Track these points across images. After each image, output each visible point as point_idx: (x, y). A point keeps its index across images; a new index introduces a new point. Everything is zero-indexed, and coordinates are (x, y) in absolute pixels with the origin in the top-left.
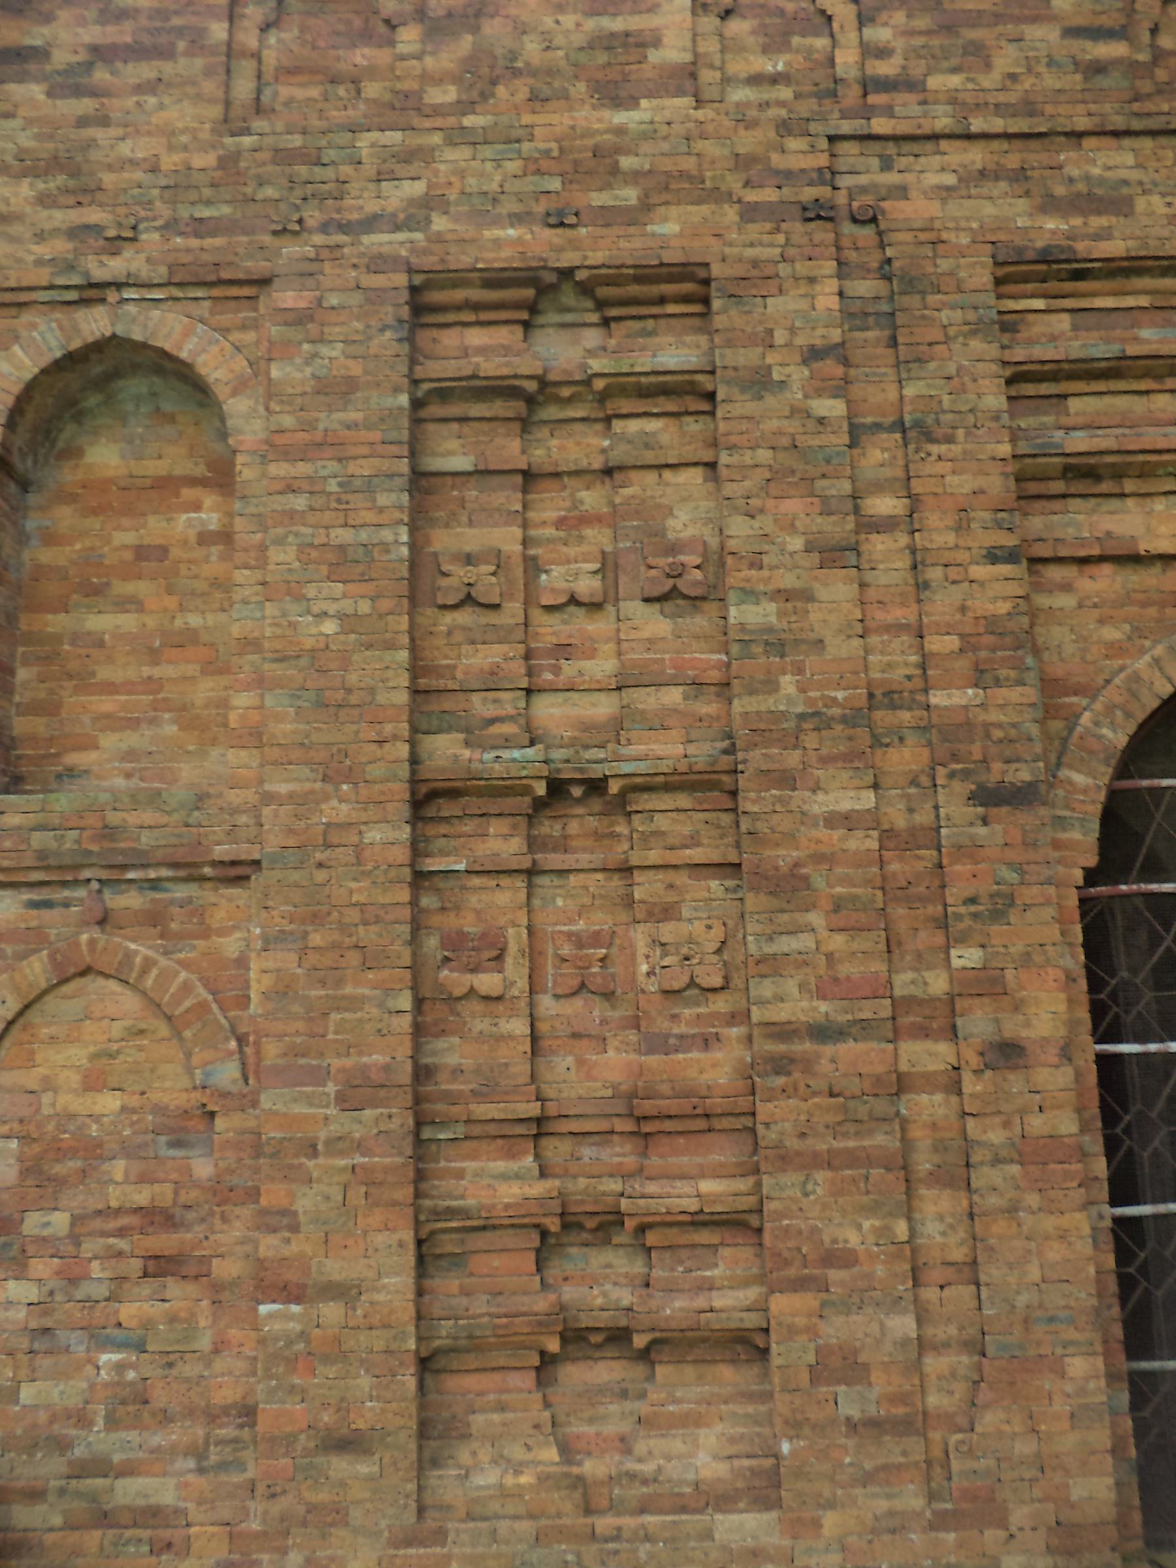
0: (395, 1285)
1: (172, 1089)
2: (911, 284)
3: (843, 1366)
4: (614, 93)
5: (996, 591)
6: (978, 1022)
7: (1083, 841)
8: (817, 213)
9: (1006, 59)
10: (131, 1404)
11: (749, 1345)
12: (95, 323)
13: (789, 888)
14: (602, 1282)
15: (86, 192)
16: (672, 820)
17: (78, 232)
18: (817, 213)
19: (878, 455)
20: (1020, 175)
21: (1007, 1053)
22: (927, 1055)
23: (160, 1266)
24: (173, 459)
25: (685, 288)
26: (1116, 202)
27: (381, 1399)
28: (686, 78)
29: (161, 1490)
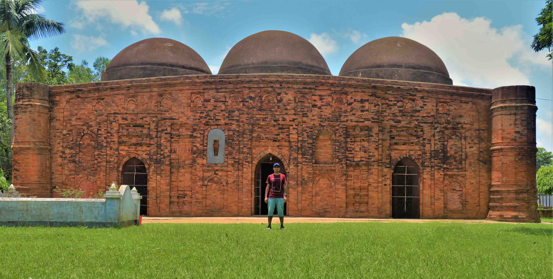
0: (345, 198)
2: (384, 128)
4: (362, 111)
5: (388, 152)
6: (384, 183)
7: (392, 171)
9: (393, 110)
10: (327, 205)
15: (321, 118)
19: (380, 142)
20: (393, 120)
21: (385, 185)
22: (379, 184)
23: (329, 196)
24: (326, 138)
26: (399, 122)
28: (367, 111)
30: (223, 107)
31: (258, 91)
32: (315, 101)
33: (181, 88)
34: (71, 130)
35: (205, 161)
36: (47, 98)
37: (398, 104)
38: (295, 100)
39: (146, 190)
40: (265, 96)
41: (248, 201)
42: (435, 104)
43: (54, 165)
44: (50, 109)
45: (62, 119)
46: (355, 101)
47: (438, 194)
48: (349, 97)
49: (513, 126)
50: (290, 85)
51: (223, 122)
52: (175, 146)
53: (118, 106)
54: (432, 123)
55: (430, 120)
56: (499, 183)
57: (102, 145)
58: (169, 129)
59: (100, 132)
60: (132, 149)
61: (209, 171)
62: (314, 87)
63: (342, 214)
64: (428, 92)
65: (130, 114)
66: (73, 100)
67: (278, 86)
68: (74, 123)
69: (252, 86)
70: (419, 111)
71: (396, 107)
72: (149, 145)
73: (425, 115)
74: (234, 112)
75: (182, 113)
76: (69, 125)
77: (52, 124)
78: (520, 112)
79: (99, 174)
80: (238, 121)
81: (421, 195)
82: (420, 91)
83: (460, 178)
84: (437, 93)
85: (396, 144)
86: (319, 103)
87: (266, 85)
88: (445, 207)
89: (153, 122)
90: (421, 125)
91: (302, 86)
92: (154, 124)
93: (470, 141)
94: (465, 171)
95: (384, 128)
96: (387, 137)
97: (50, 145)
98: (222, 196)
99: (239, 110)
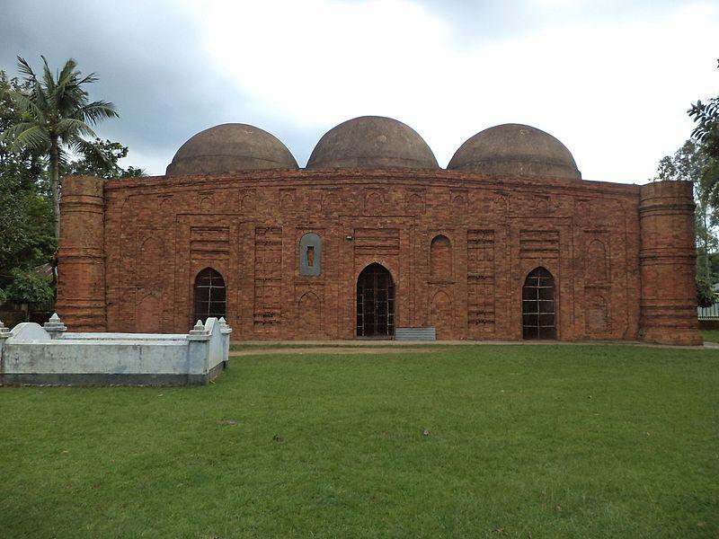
0: (466, 316)
1: (448, 300)
2: (512, 232)
3: (501, 323)
4: (487, 212)
5: (518, 261)
7: (523, 283)
8: (504, 225)
9: (523, 209)
11: (493, 322)
12: (439, 233)
13: (498, 286)
14: (481, 317)
15: (437, 220)
16: (489, 279)
17: (438, 224)
18: (504, 225)
20: (523, 222)
21: (515, 300)
22: (508, 300)
23: (448, 314)
25: (493, 231)
27: (465, 324)
29: (449, 331)
30: (319, 207)
31: (362, 187)
32: (429, 200)
33: (267, 184)
34: (131, 234)
35: (297, 273)
36: (100, 193)
37: (529, 203)
38: (406, 199)
39: (225, 307)
40: (369, 194)
41: (350, 321)
42: (573, 203)
43: (108, 276)
44: (105, 208)
45: (120, 220)
46: (477, 200)
47: (579, 311)
48: (470, 195)
49: (670, 229)
50: (400, 181)
51: (318, 225)
52: (260, 254)
53: (188, 205)
54: (569, 226)
55: (568, 222)
56: (655, 297)
57: (169, 254)
58: (253, 233)
59: (167, 237)
60: (207, 257)
61: (301, 284)
62: (427, 183)
63: (463, 335)
64: (563, 188)
65: (204, 215)
66: (133, 197)
67: (385, 181)
68: (134, 225)
69: (353, 181)
70: (554, 212)
71: (526, 207)
72: (227, 253)
73: (561, 216)
74: (331, 213)
75: (270, 214)
76: (128, 230)
77: (107, 226)
78: (678, 212)
79: (166, 289)
80: (337, 224)
81: (558, 312)
82: (556, 188)
83: (604, 292)
84: (575, 189)
85: (527, 251)
86: (434, 203)
87: (370, 181)
88: (587, 326)
89: (234, 224)
90: (557, 228)
91: (413, 183)
92: (234, 227)
93: (615, 246)
94: (610, 283)
95: (512, 232)
96: (516, 242)
97: (104, 252)
98: (318, 315)
99: (337, 211)
